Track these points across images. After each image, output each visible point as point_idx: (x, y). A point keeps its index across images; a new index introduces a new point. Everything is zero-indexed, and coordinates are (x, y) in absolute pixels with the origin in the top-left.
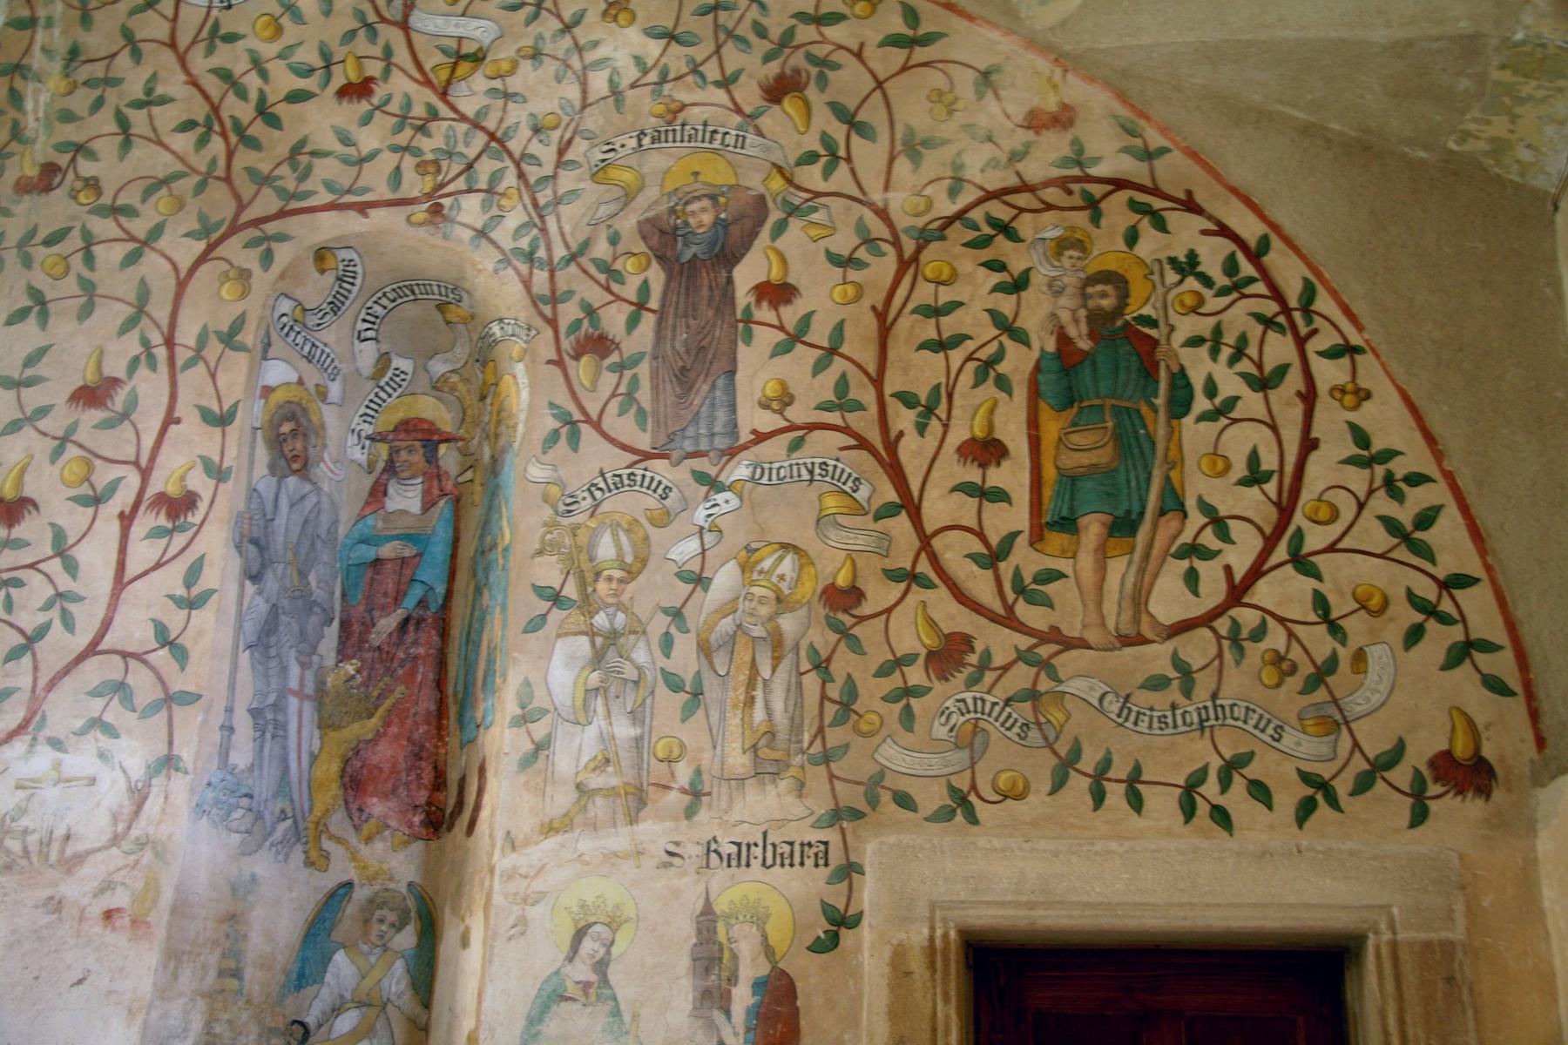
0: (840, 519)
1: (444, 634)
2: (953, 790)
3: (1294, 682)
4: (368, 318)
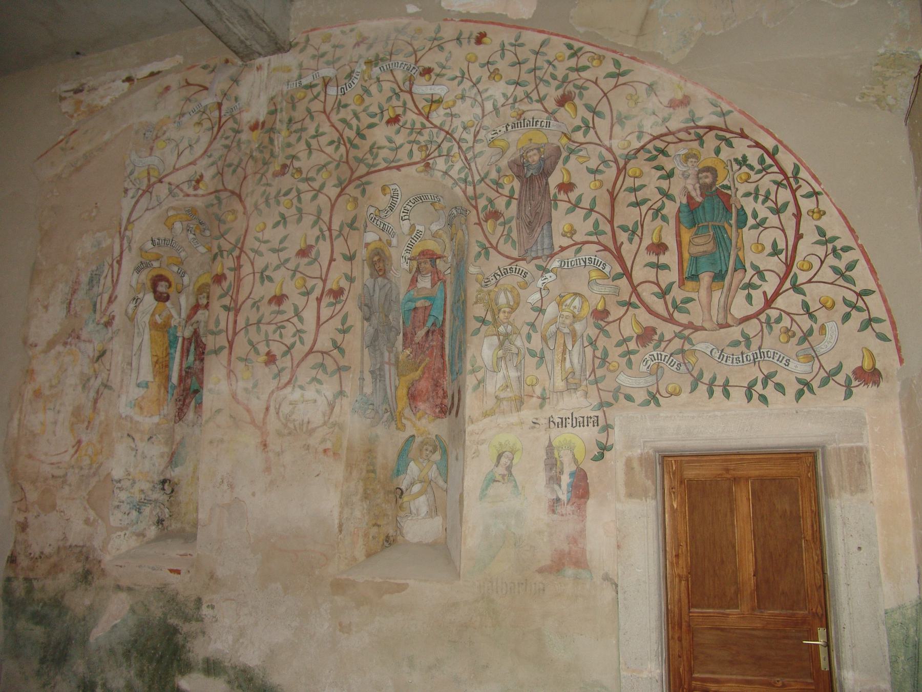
0: (598, 281)
1: (443, 336)
2: (649, 393)
3: (794, 340)
4: (405, 211)
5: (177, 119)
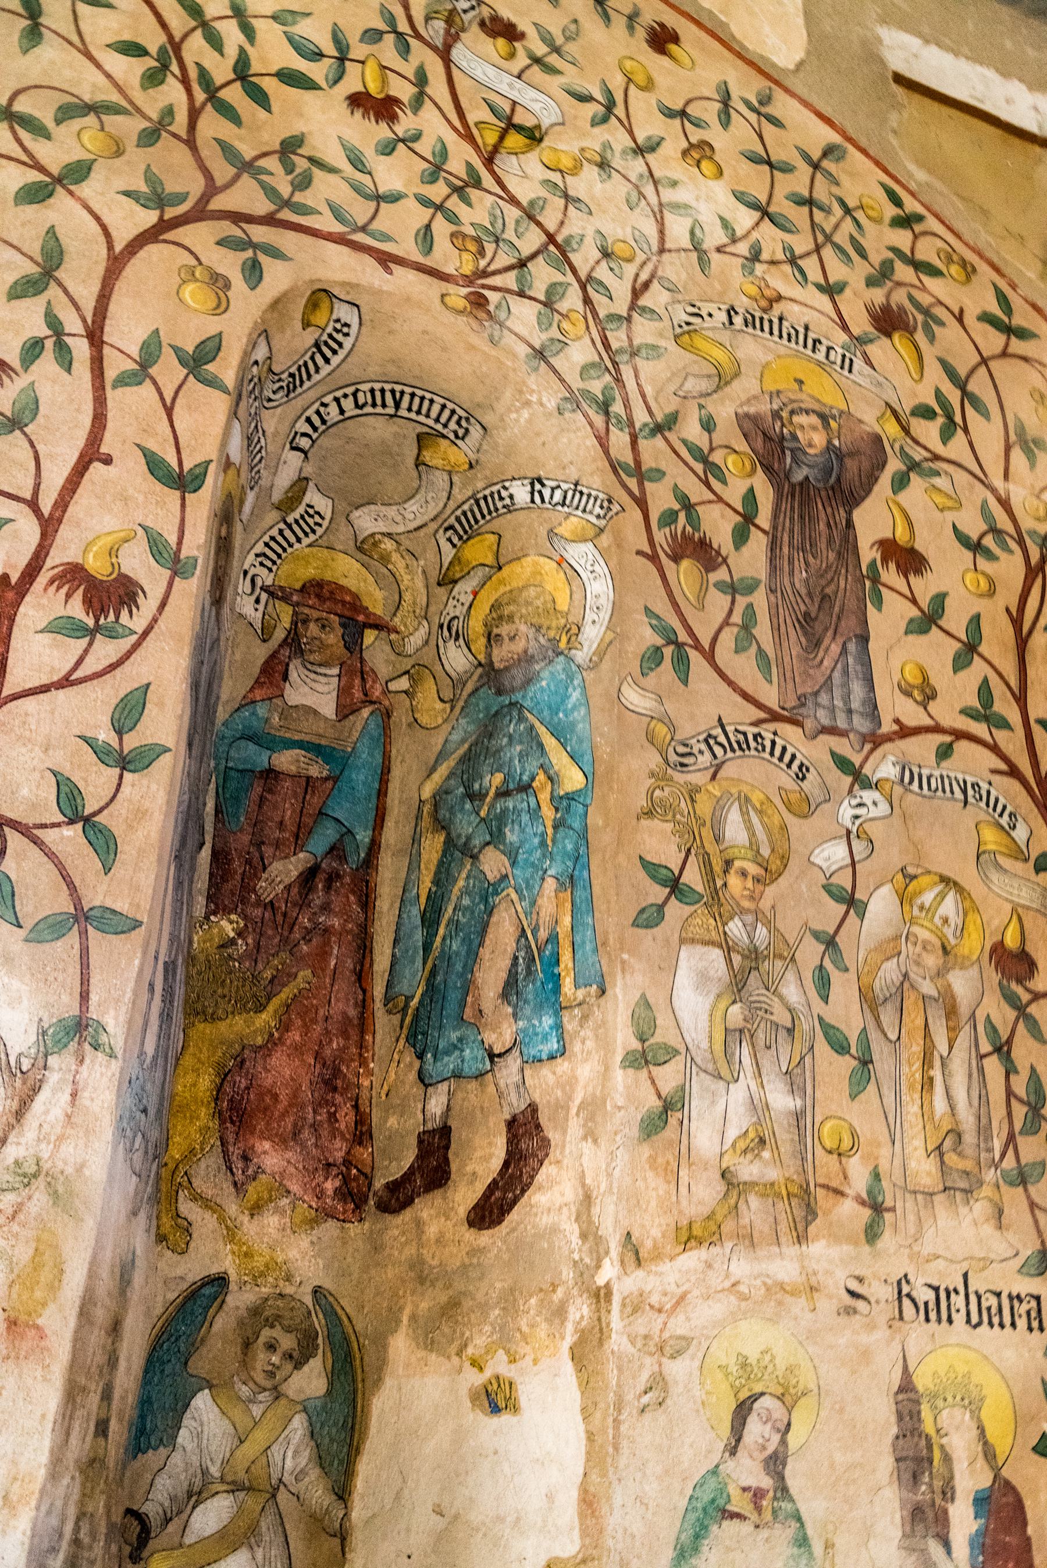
0: (1001, 859)
1: (367, 901)
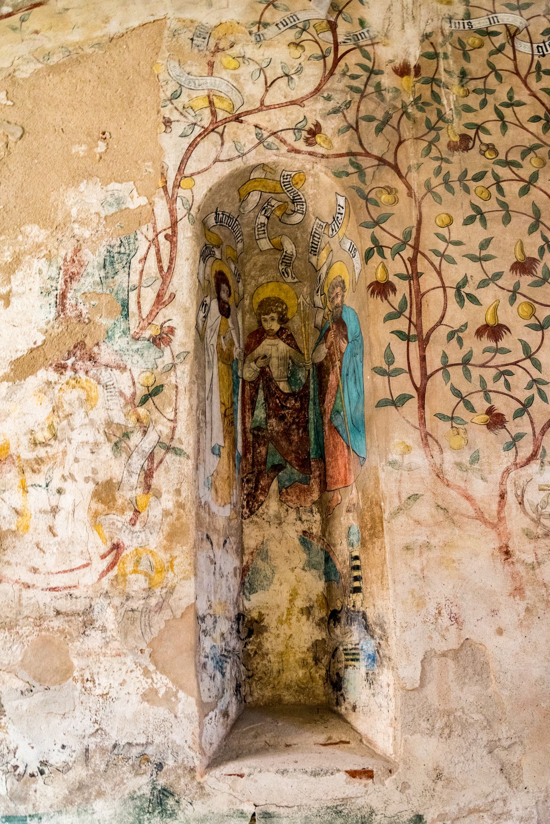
5: (255, 29)
